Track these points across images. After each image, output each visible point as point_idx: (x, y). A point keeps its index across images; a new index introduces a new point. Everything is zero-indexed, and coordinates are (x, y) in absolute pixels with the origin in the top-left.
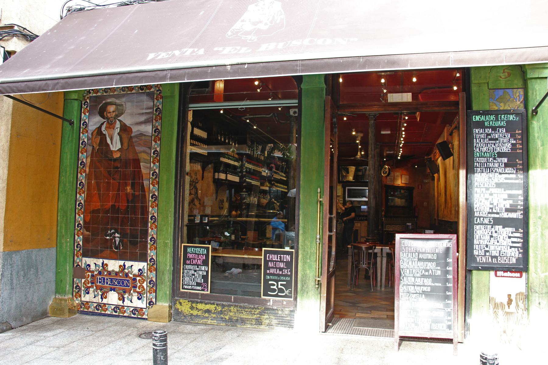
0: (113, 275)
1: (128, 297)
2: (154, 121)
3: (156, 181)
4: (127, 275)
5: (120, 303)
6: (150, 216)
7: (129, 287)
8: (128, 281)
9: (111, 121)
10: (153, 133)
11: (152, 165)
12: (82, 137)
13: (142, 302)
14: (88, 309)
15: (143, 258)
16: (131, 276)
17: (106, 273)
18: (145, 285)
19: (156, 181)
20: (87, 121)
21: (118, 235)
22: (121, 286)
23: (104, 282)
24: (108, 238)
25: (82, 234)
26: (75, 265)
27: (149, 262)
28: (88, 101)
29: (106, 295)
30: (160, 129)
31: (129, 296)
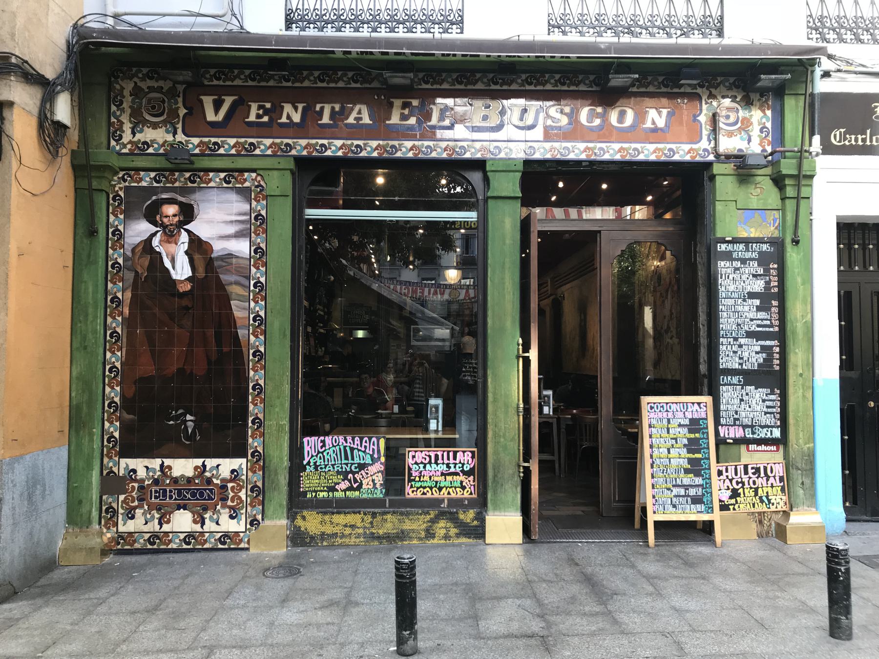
0: (182, 483)
1: (211, 517)
2: (253, 235)
3: (261, 330)
4: (209, 481)
5: (197, 528)
6: (251, 385)
7: (213, 500)
8: (211, 490)
9: (170, 231)
10: (253, 254)
11: (252, 304)
12: (113, 255)
13: (238, 523)
14: (132, 545)
15: (239, 451)
16: (215, 481)
17: (168, 482)
18: (242, 494)
19: (261, 330)
20: (121, 228)
21: (192, 418)
22: (197, 499)
23: (165, 495)
24: (171, 422)
25: (119, 419)
26: (105, 473)
27: (250, 457)
28: (122, 194)
29: (168, 517)
30: (265, 249)
31: (214, 514)
